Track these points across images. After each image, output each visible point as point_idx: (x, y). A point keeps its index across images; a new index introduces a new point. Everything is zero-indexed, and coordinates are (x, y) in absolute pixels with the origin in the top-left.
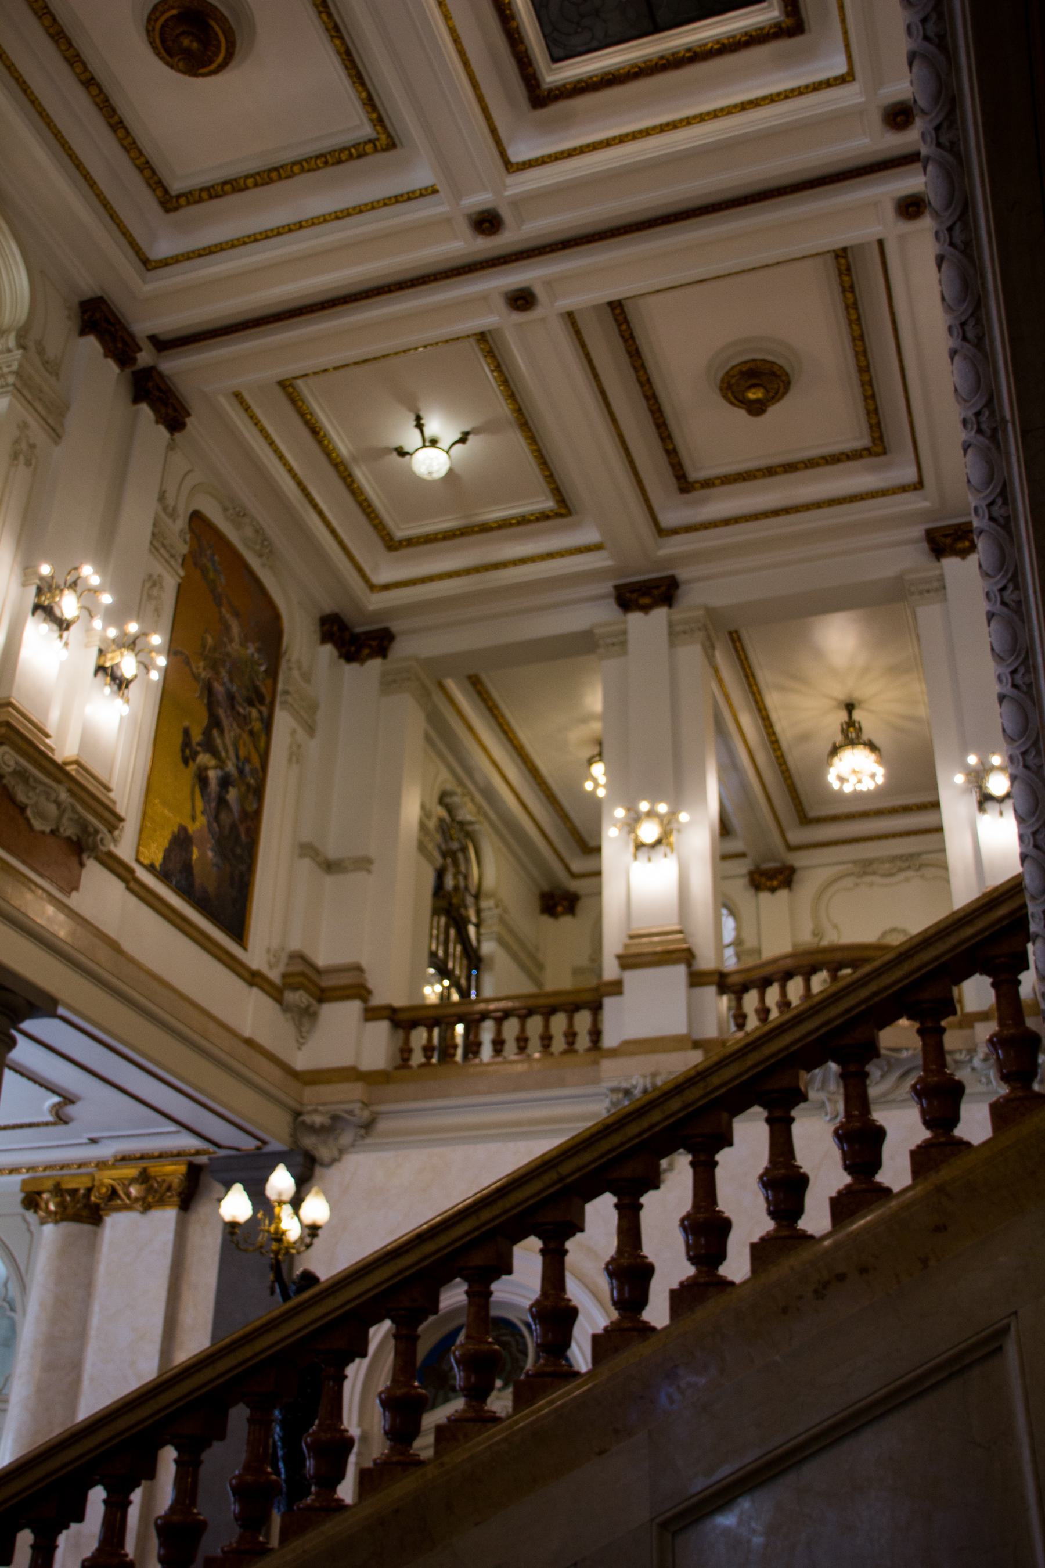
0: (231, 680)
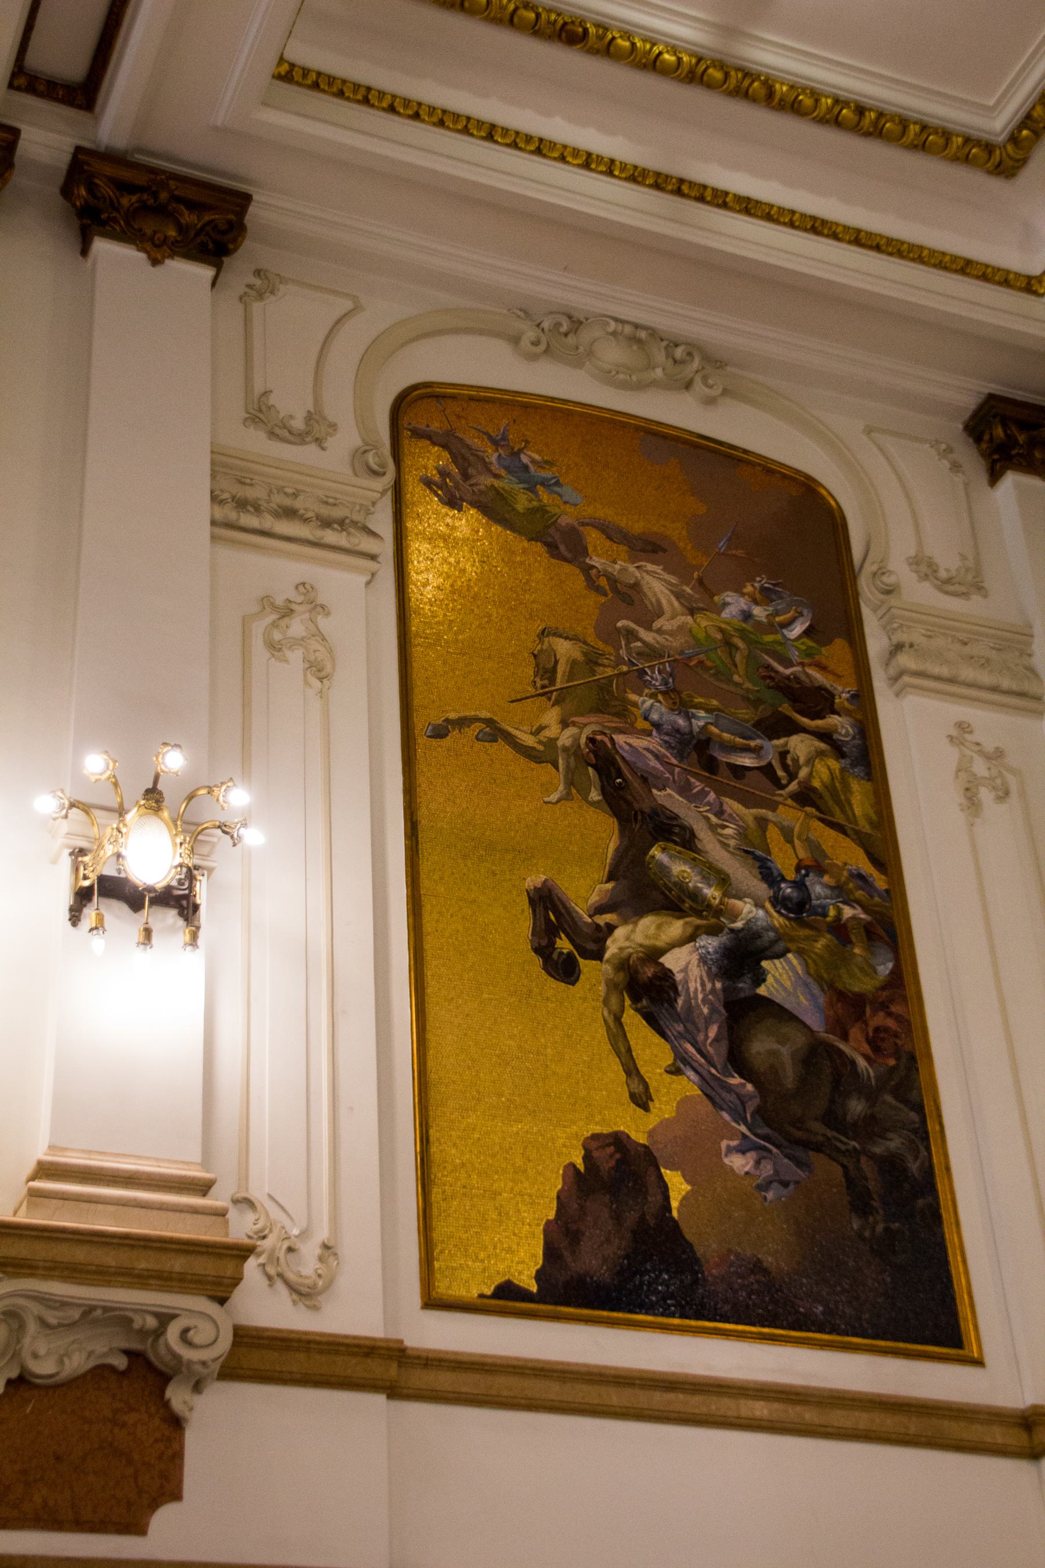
0: (683, 707)
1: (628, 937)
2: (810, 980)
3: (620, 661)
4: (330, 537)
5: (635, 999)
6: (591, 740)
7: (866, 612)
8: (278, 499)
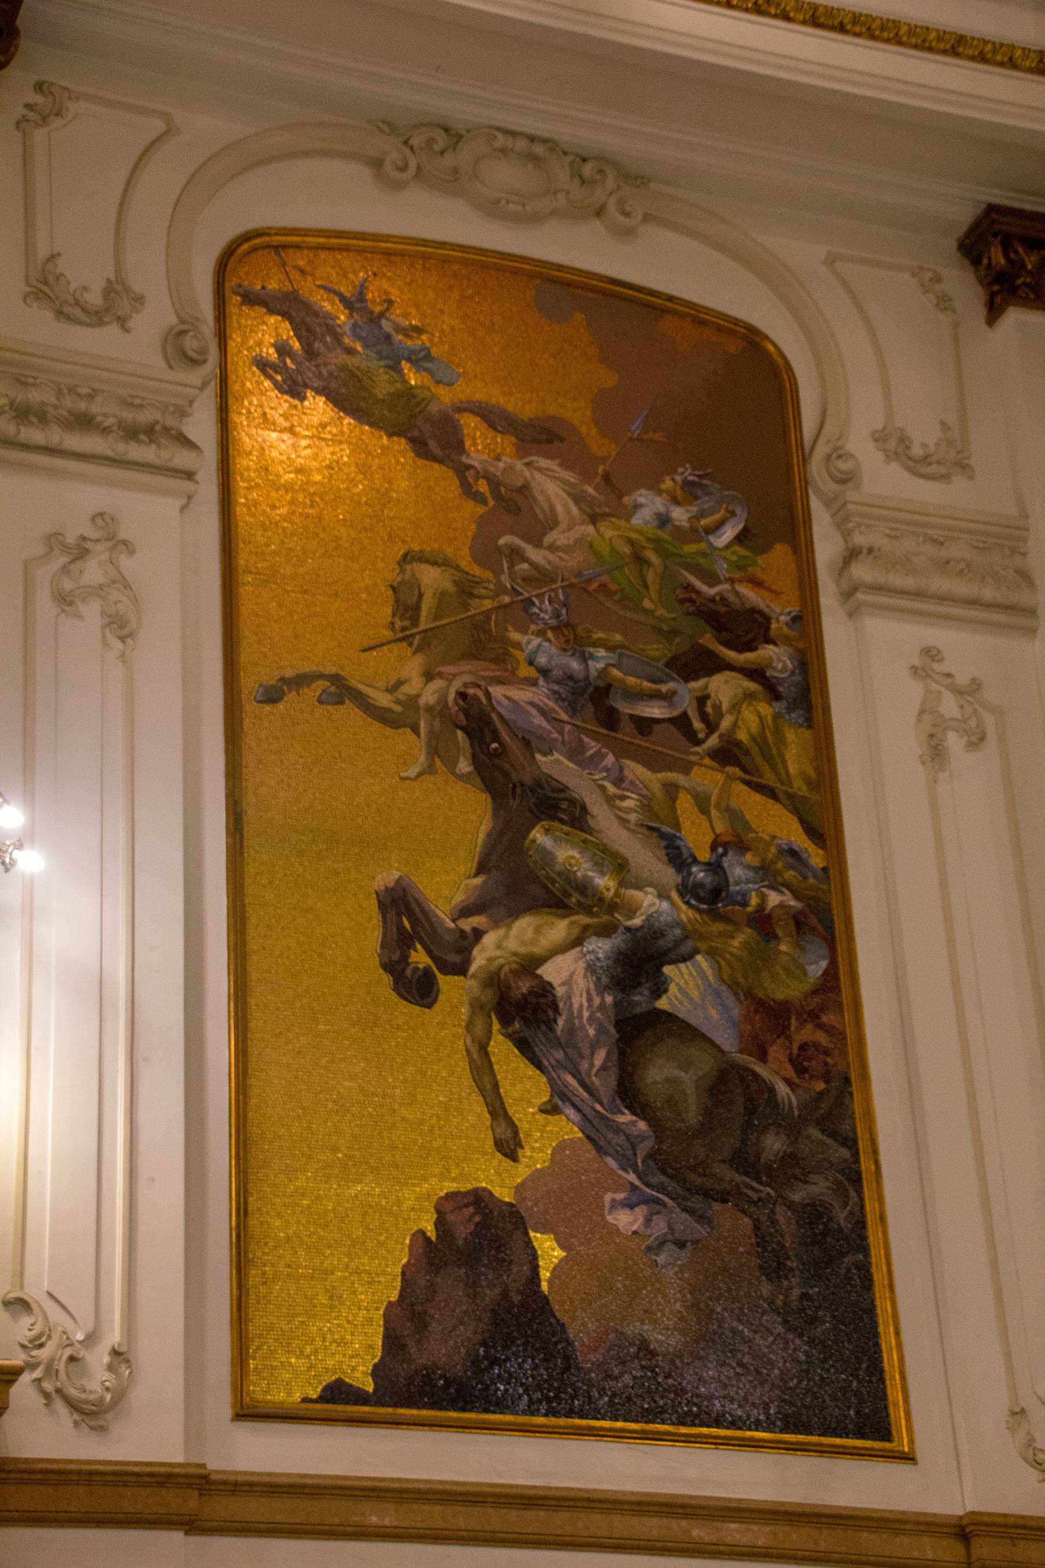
1: (498, 945)
2: (724, 988)
3: (501, 590)
4: (135, 451)
5: (506, 1021)
6: (462, 695)
7: (816, 505)
8: (68, 402)
